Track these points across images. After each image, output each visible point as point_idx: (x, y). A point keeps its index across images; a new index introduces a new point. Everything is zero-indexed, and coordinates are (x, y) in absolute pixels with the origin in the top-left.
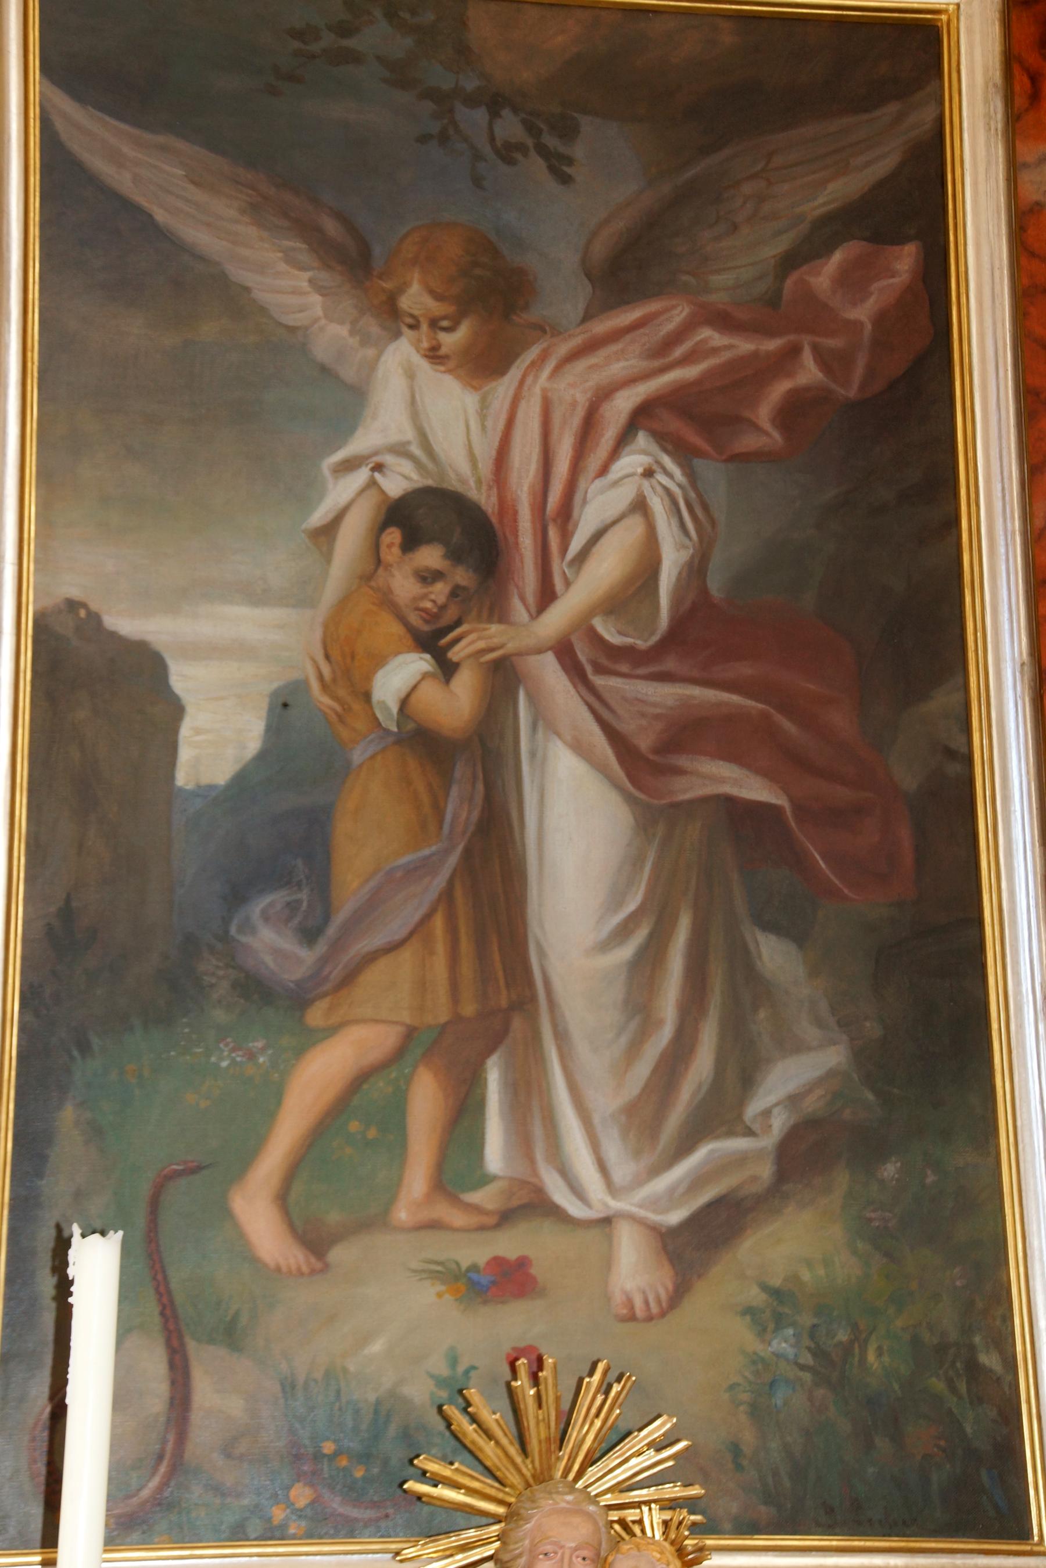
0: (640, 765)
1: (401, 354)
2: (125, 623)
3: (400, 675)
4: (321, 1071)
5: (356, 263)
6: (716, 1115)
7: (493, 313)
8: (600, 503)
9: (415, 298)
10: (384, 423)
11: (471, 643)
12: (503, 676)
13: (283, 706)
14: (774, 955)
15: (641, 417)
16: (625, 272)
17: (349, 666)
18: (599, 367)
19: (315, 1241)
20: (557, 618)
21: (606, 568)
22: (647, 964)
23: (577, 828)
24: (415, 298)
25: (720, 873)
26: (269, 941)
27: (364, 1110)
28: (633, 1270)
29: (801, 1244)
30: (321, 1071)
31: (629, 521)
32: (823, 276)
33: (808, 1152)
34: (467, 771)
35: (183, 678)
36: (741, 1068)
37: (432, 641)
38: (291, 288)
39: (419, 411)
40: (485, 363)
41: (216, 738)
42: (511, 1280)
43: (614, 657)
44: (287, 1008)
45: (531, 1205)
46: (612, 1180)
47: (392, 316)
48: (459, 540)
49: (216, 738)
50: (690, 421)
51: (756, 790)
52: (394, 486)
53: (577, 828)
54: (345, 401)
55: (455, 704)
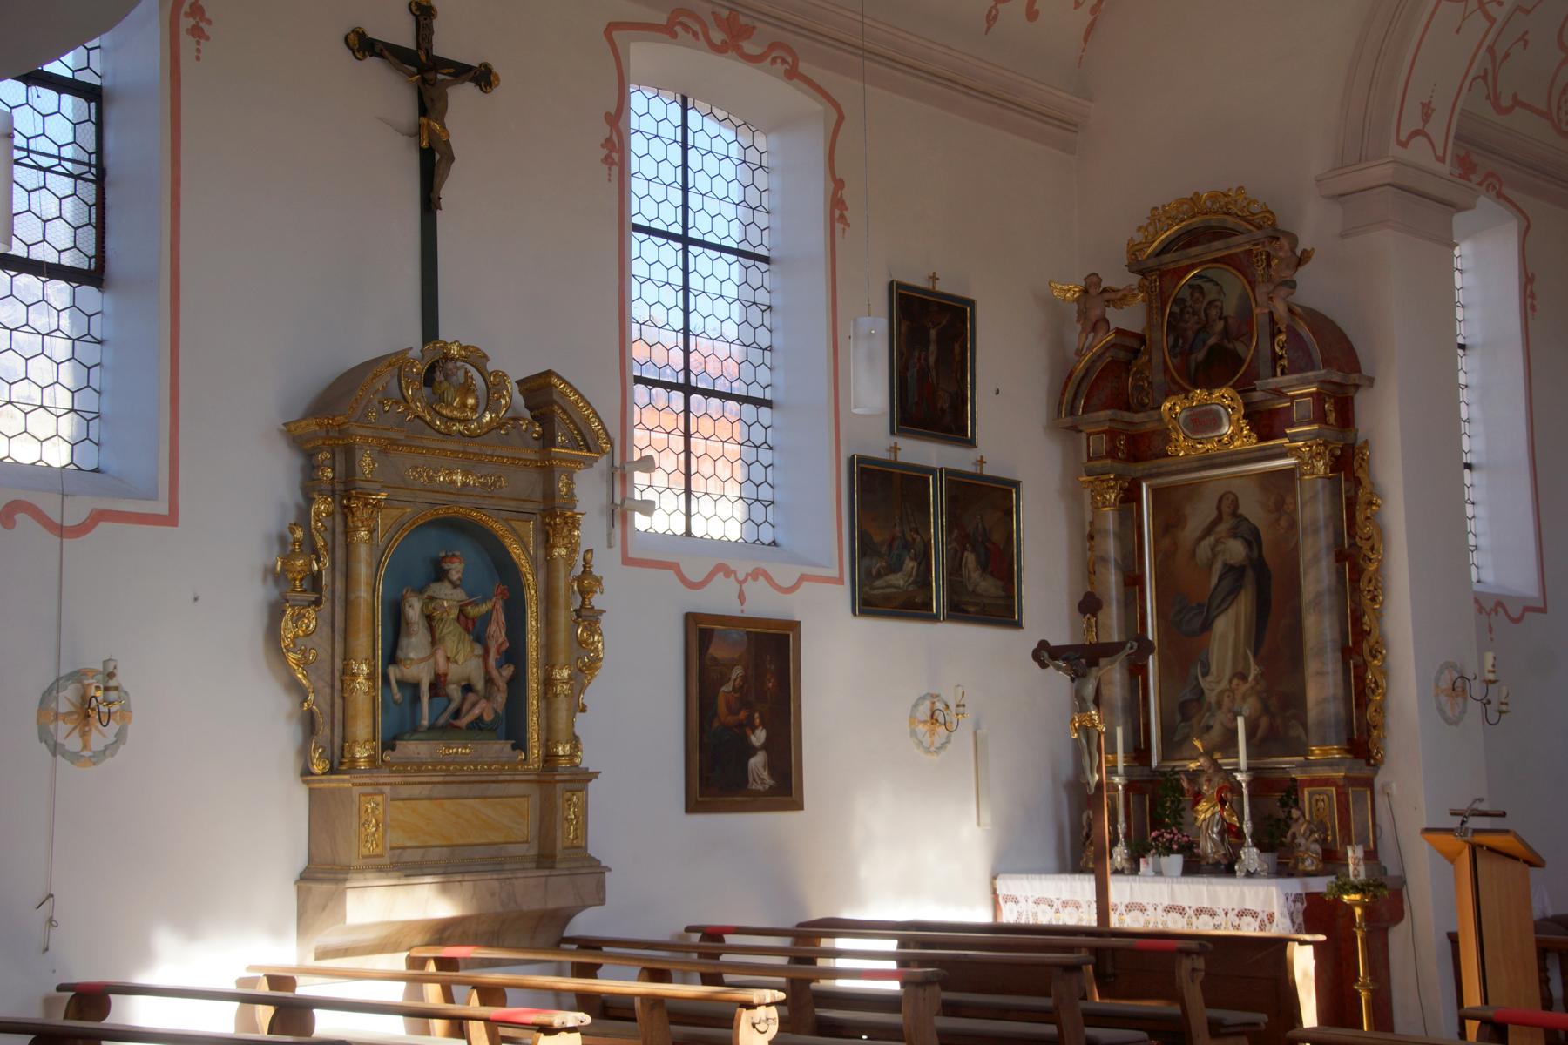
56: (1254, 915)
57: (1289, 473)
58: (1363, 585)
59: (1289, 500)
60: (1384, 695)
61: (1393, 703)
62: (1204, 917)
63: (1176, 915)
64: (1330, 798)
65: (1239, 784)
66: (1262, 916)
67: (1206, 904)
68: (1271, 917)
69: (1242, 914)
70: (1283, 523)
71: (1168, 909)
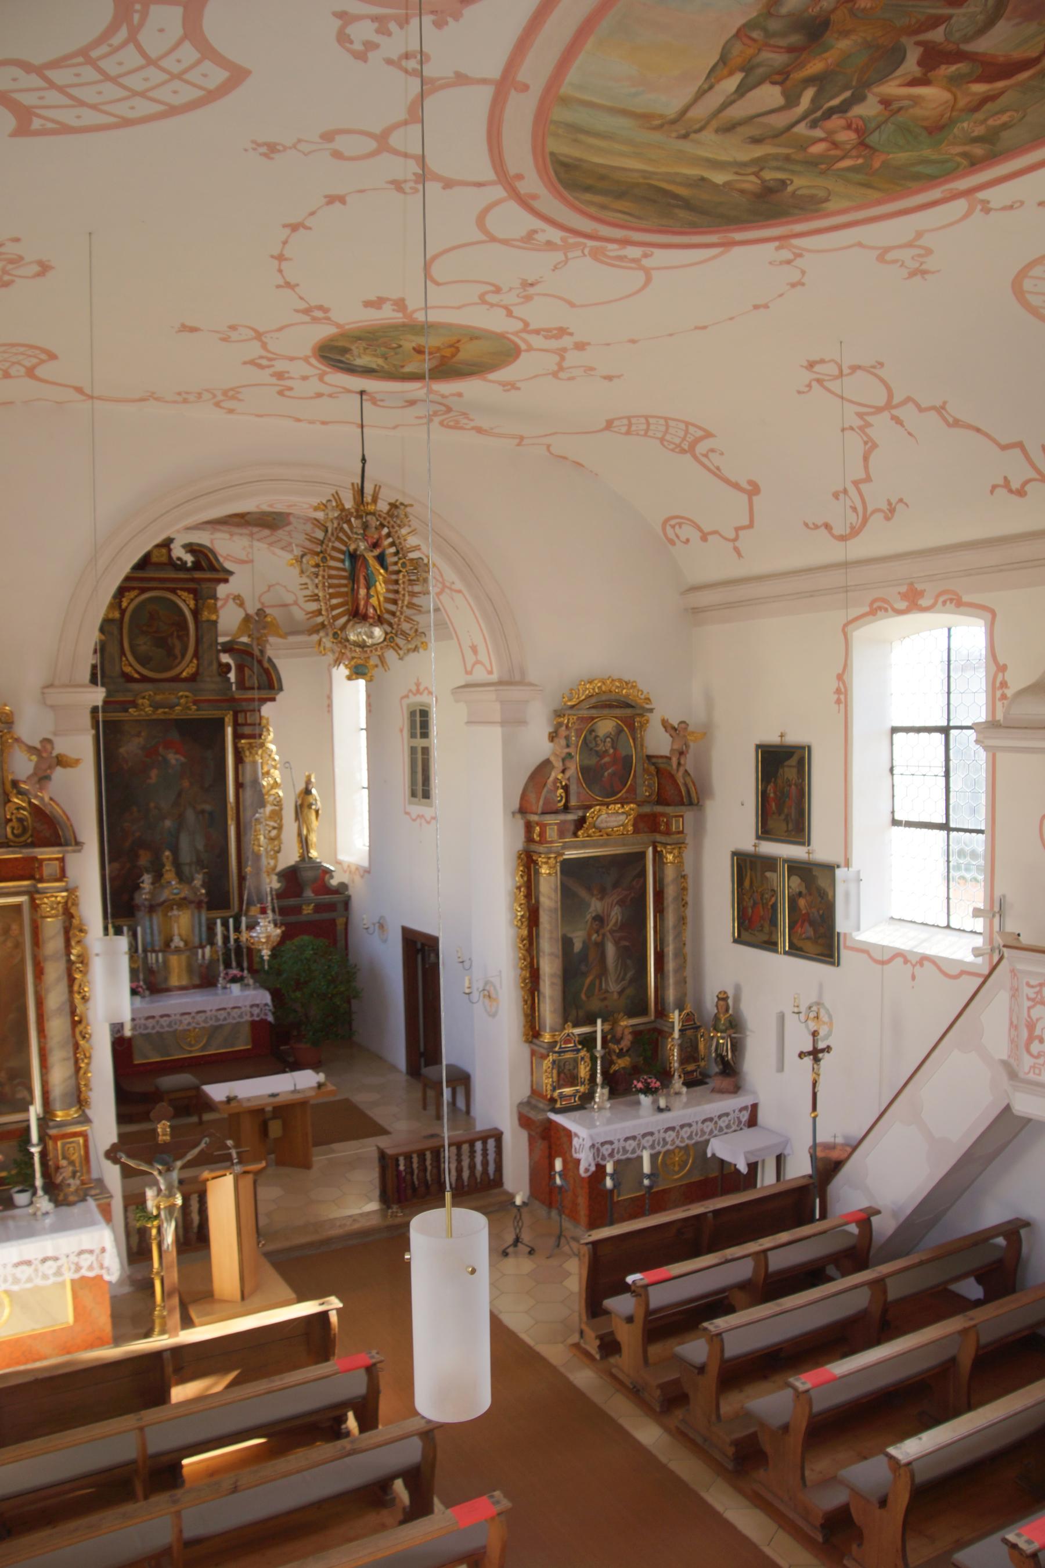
0: (616, 943)
1: (594, 899)
2: (569, 935)
3: (594, 937)
4: (588, 981)
5: (589, 889)
6: (623, 979)
7: (603, 893)
8: (613, 913)
9: (595, 892)
10: (592, 909)
11: (602, 931)
12: (604, 935)
13: (584, 942)
14: (629, 962)
15: (617, 903)
16: (615, 885)
17: (589, 936)
18: (614, 897)
19: (588, 997)
20: (609, 928)
21: (613, 921)
22: (616, 966)
23: (611, 950)
24: (595, 892)
25: (624, 953)
26: (583, 968)
27: (592, 983)
28: (616, 996)
29: (630, 991)
30: (588, 981)
31: (616, 915)
32: (634, 883)
33: (631, 981)
34: (601, 946)
35: (575, 940)
36: (625, 974)
37: (597, 932)
38: (583, 893)
39: (596, 906)
40: (601, 899)
41: (578, 946)
42: (605, 999)
43: (615, 931)
44: (585, 975)
45: (607, 991)
46: (613, 987)
47: (593, 895)
48: (599, 919)
49: (578, 946)
50: (621, 903)
51: (627, 943)
52: (594, 915)
53: (611, 950)
54: (589, 905)
55: (599, 939)
56: (91, 1252)
57: (18, 908)
58: (76, 988)
59: (15, 927)
60: (88, 1064)
61: (94, 1066)
62: (50, 1263)
63: (24, 1267)
64: (79, 1143)
65: (32, 1154)
66: (97, 1251)
67: (50, 1254)
68: (103, 1250)
69: (81, 1252)
70: (10, 944)
71: (17, 1265)
